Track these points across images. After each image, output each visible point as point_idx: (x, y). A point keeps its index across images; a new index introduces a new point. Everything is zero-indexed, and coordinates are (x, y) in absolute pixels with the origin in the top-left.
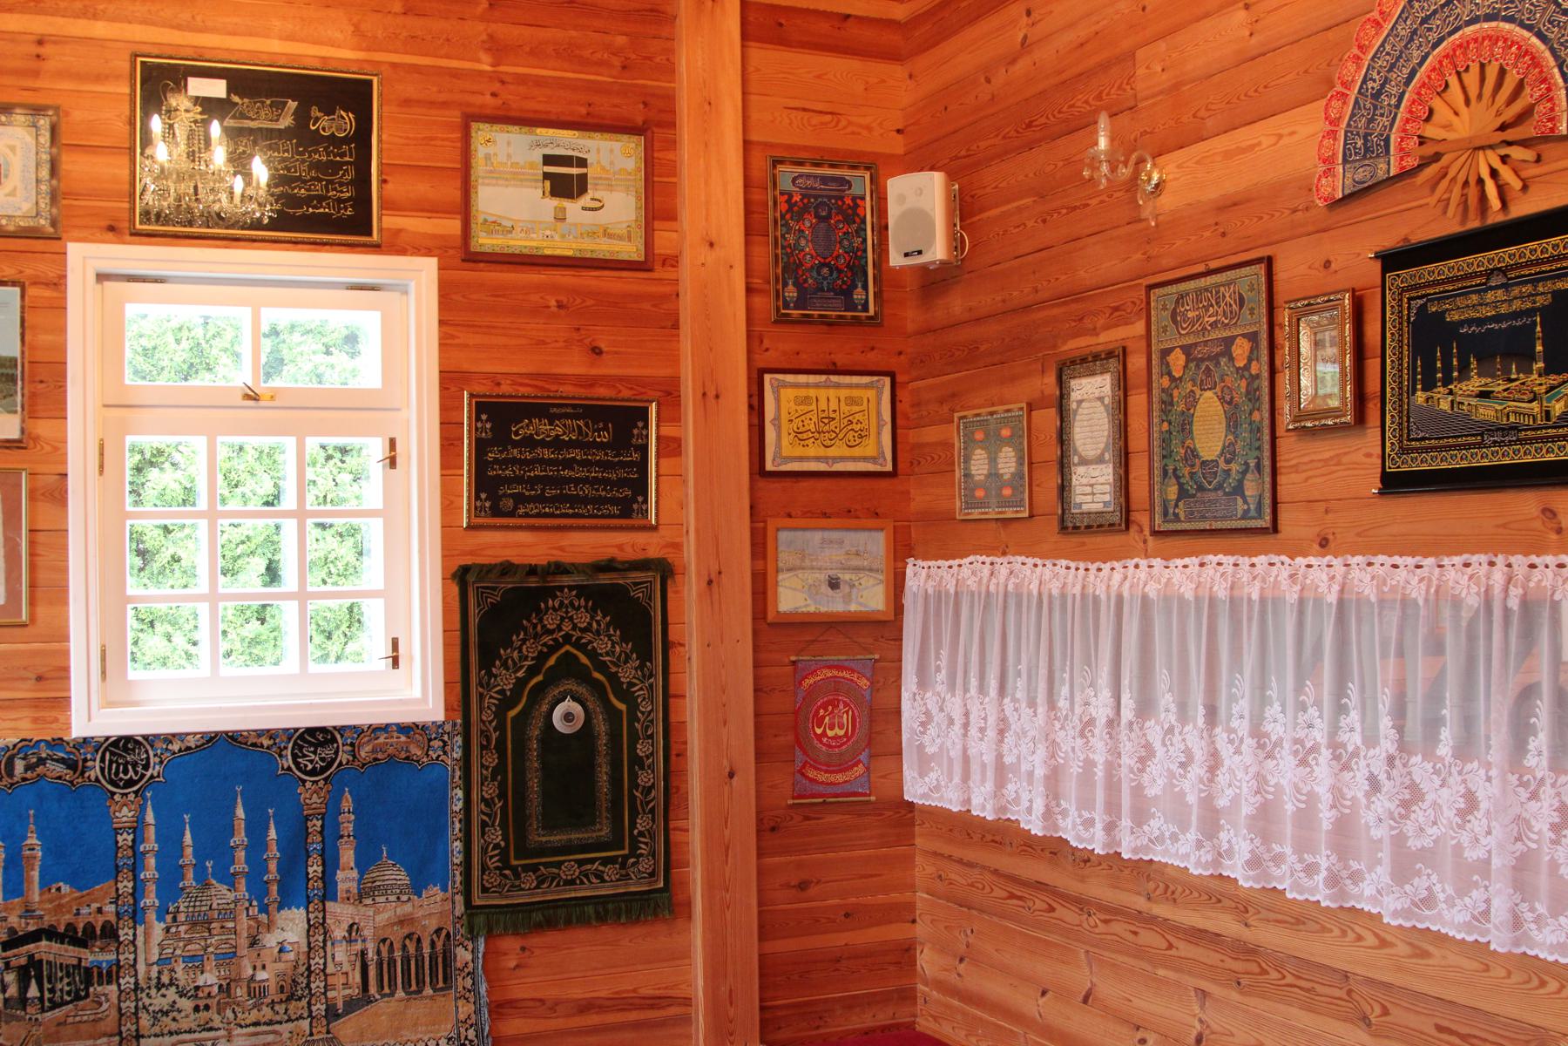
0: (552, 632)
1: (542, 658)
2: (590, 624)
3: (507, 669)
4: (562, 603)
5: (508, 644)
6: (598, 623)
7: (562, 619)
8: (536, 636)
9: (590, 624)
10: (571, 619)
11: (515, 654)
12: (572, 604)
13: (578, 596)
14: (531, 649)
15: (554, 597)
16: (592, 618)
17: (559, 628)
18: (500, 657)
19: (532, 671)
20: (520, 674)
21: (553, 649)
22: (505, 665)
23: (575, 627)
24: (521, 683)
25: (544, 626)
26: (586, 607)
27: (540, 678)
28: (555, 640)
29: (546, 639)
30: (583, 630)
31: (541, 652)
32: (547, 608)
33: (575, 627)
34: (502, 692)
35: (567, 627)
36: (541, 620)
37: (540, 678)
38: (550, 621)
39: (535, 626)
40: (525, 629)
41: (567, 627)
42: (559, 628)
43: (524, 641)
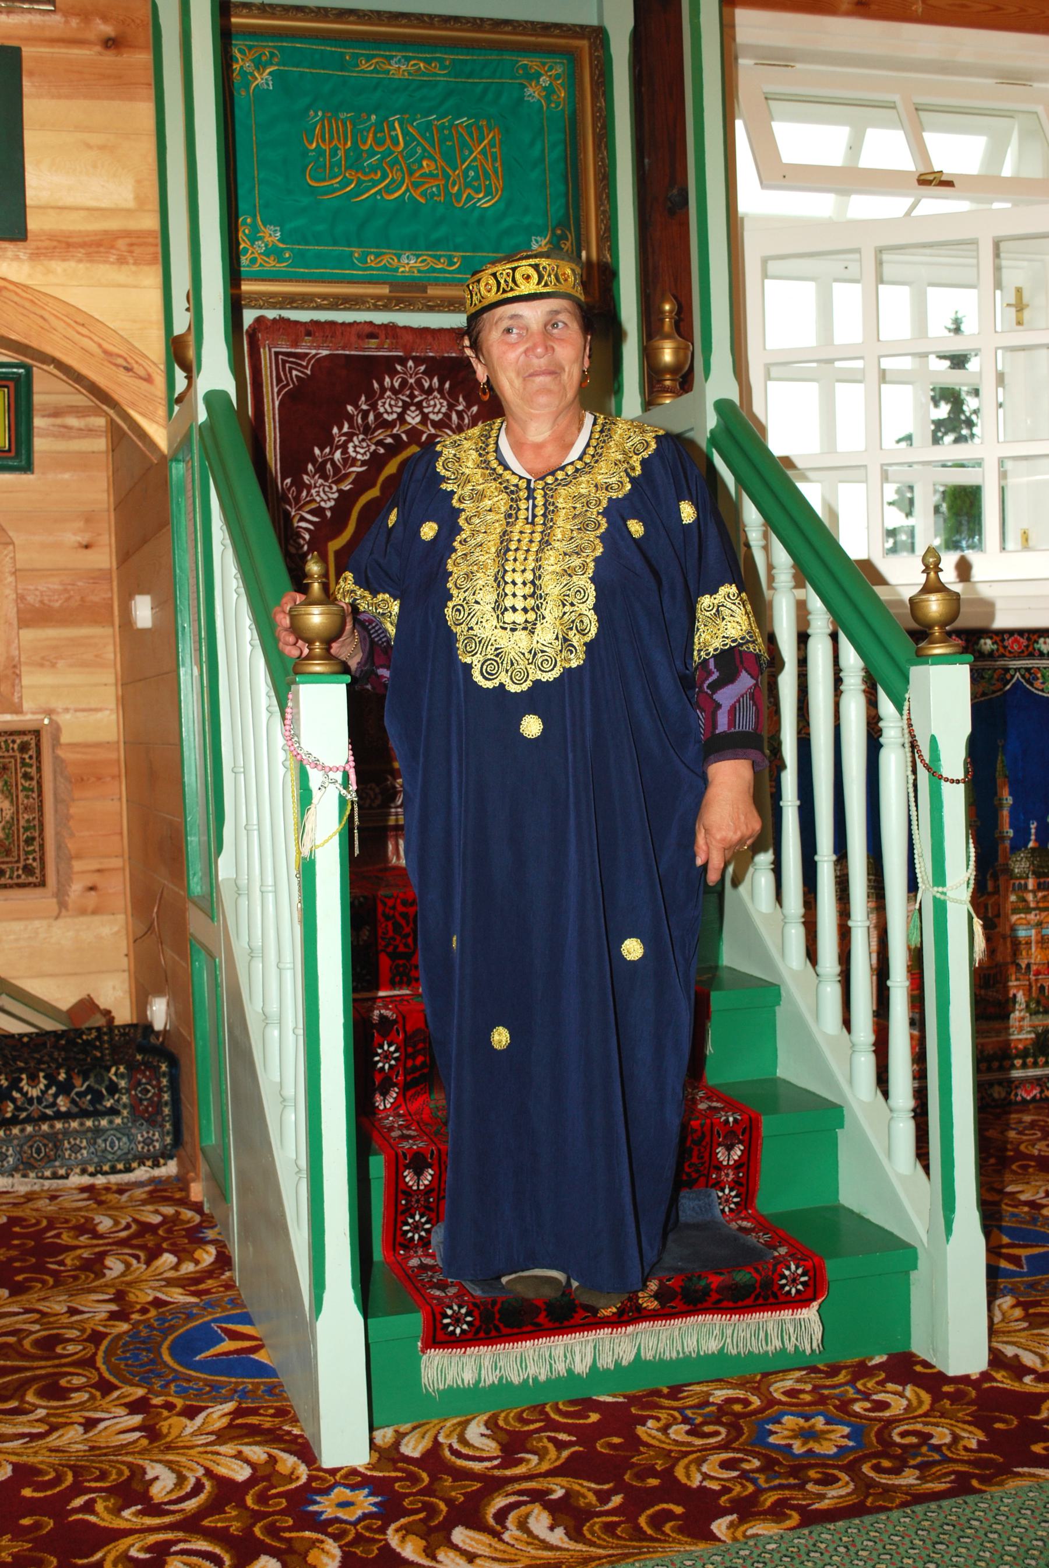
0: (391, 425)
1: (376, 463)
2: (447, 416)
3: (325, 477)
4: (404, 383)
5: (327, 441)
6: (460, 415)
7: (406, 406)
8: (367, 430)
9: (447, 416)
10: (419, 406)
11: (338, 455)
12: (419, 382)
13: (428, 373)
14: (360, 450)
15: (393, 373)
16: (451, 407)
17: (401, 418)
18: (314, 460)
19: (363, 483)
20: (346, 486)
21: (393, 450)
22: (321, 470)
23: (425, 418)
24: (345, 501)
25: (379, 416)
26: (440, 390)
27: (374, 493)
28: (396, 437)
29: (380, 435)
30: (435, 424)
31: (374, 454)
32: (383, 390)
33: (425, 418)
34: (319, 512)
35: (413, 418)
36: (374, 406)
37: (374, 493)
38: (389, 408)
39: (365, 414)
40: (350, 418)
41: (413, 418)
42: (401, 418)
43: (350, 436)
